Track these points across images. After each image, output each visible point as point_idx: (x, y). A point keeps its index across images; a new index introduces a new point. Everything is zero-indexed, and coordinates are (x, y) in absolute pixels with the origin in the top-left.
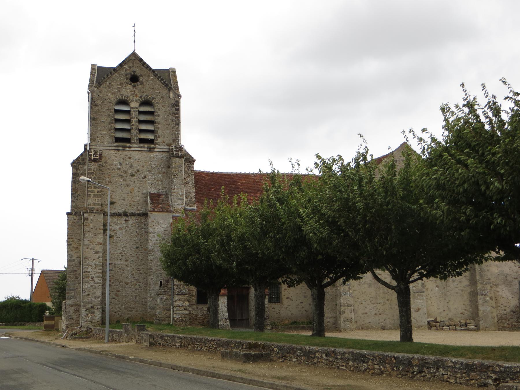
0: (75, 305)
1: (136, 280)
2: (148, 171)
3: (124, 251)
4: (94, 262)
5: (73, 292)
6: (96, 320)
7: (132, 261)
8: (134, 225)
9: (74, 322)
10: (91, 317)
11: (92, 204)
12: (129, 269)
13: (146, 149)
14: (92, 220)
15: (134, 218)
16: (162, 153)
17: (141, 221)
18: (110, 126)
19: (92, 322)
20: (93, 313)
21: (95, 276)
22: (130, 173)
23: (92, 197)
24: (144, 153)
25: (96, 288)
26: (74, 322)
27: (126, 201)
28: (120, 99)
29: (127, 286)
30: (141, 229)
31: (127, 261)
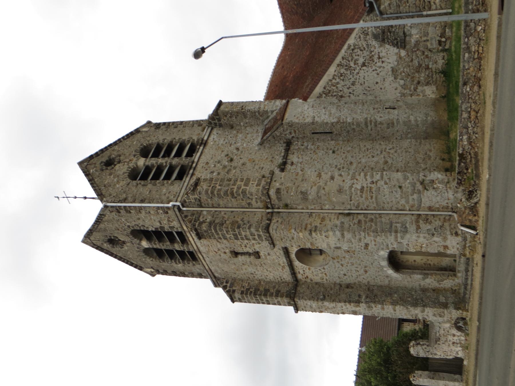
0: (417, 221)
1: (381, 152)
2: (230, 146)
3: (336, 166)
4: (346, 181)
5: (394, 225)
6: (444, 177)
7: (352, 157)
8: (300, 156)
9: (446, 224)
10: (439, 183)
11: (258, 187)
12: (363, 161)
13: (202, 148)
14: (282, 184)
15: (290, 156)
16: (212, 134)
17: (296, 150)
18: (158, 185)
19: (448, 182)
20: (433, 181)
21: (369, 180)
22: (227, 163)
23: (248, 188)
24: (206, 150)
25: (389, 179)
26: (446, 224)
27: (264, 166)
28: (128, 175)
29: (390, 161)
30: (307, 149)
31: (351, 163)
